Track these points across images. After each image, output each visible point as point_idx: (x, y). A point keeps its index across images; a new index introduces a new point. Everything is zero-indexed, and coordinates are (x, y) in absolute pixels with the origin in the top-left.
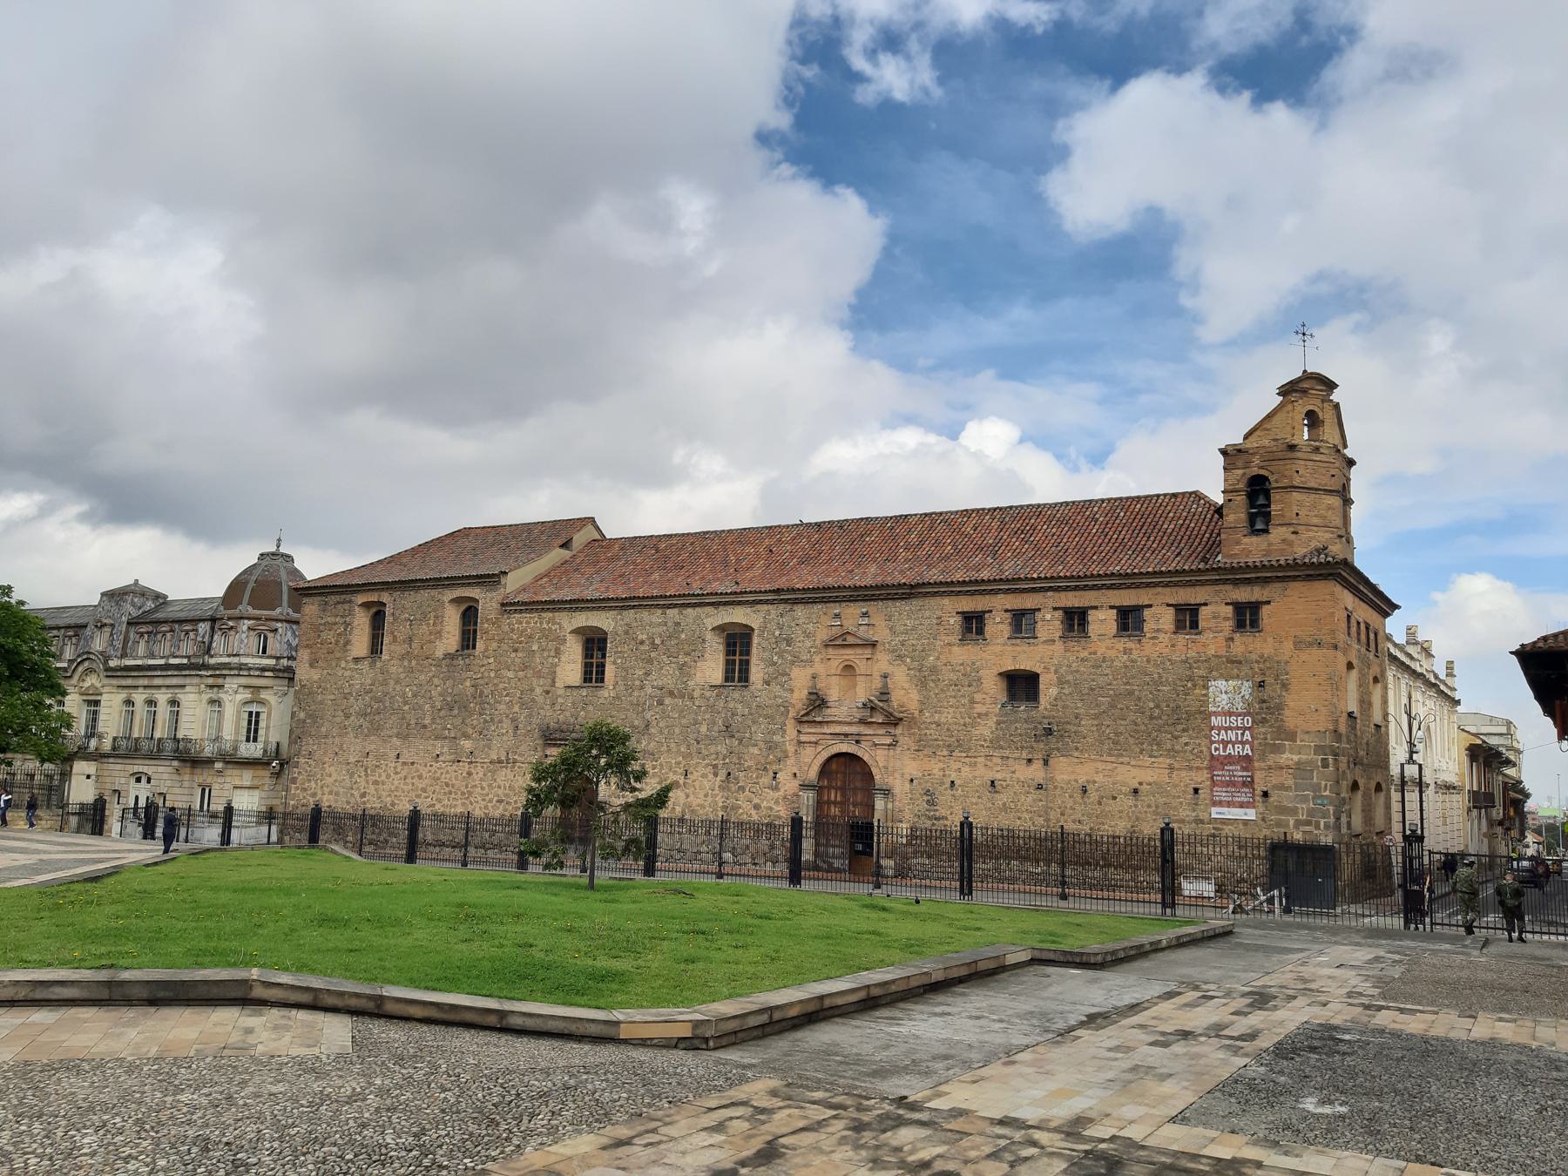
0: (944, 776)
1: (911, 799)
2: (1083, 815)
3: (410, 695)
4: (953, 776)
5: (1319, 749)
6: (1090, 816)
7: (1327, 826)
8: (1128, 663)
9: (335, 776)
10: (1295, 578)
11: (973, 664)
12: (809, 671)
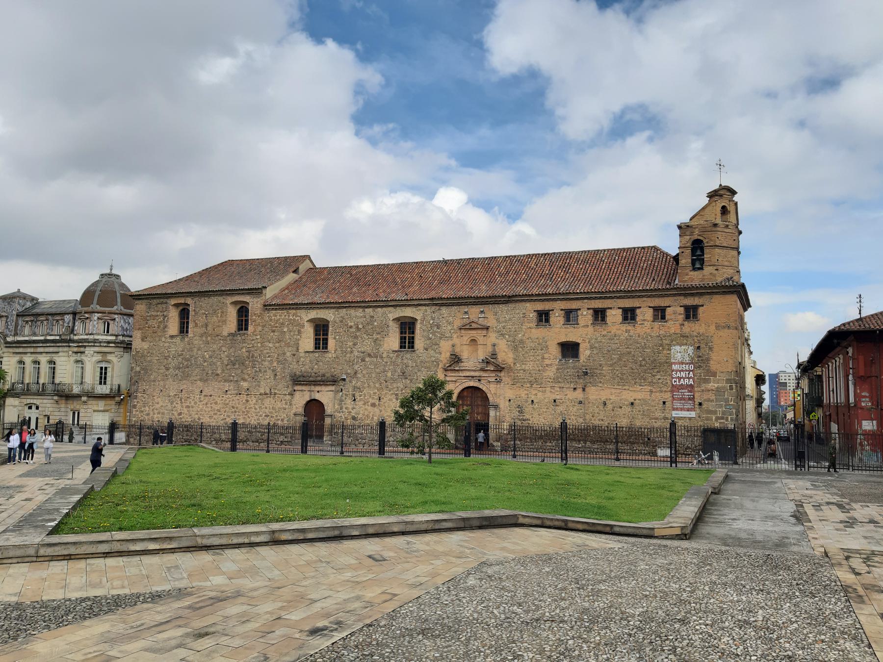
2: (604, 417)
3: (207, 356)
4: (533, 398)
5: (728, 381)
6: (607, 417)
7: (732, 419)
8: (628, 337)
9: (161, 404)
10: (716, 293)
11: (544, 338)
12: (450, 343)
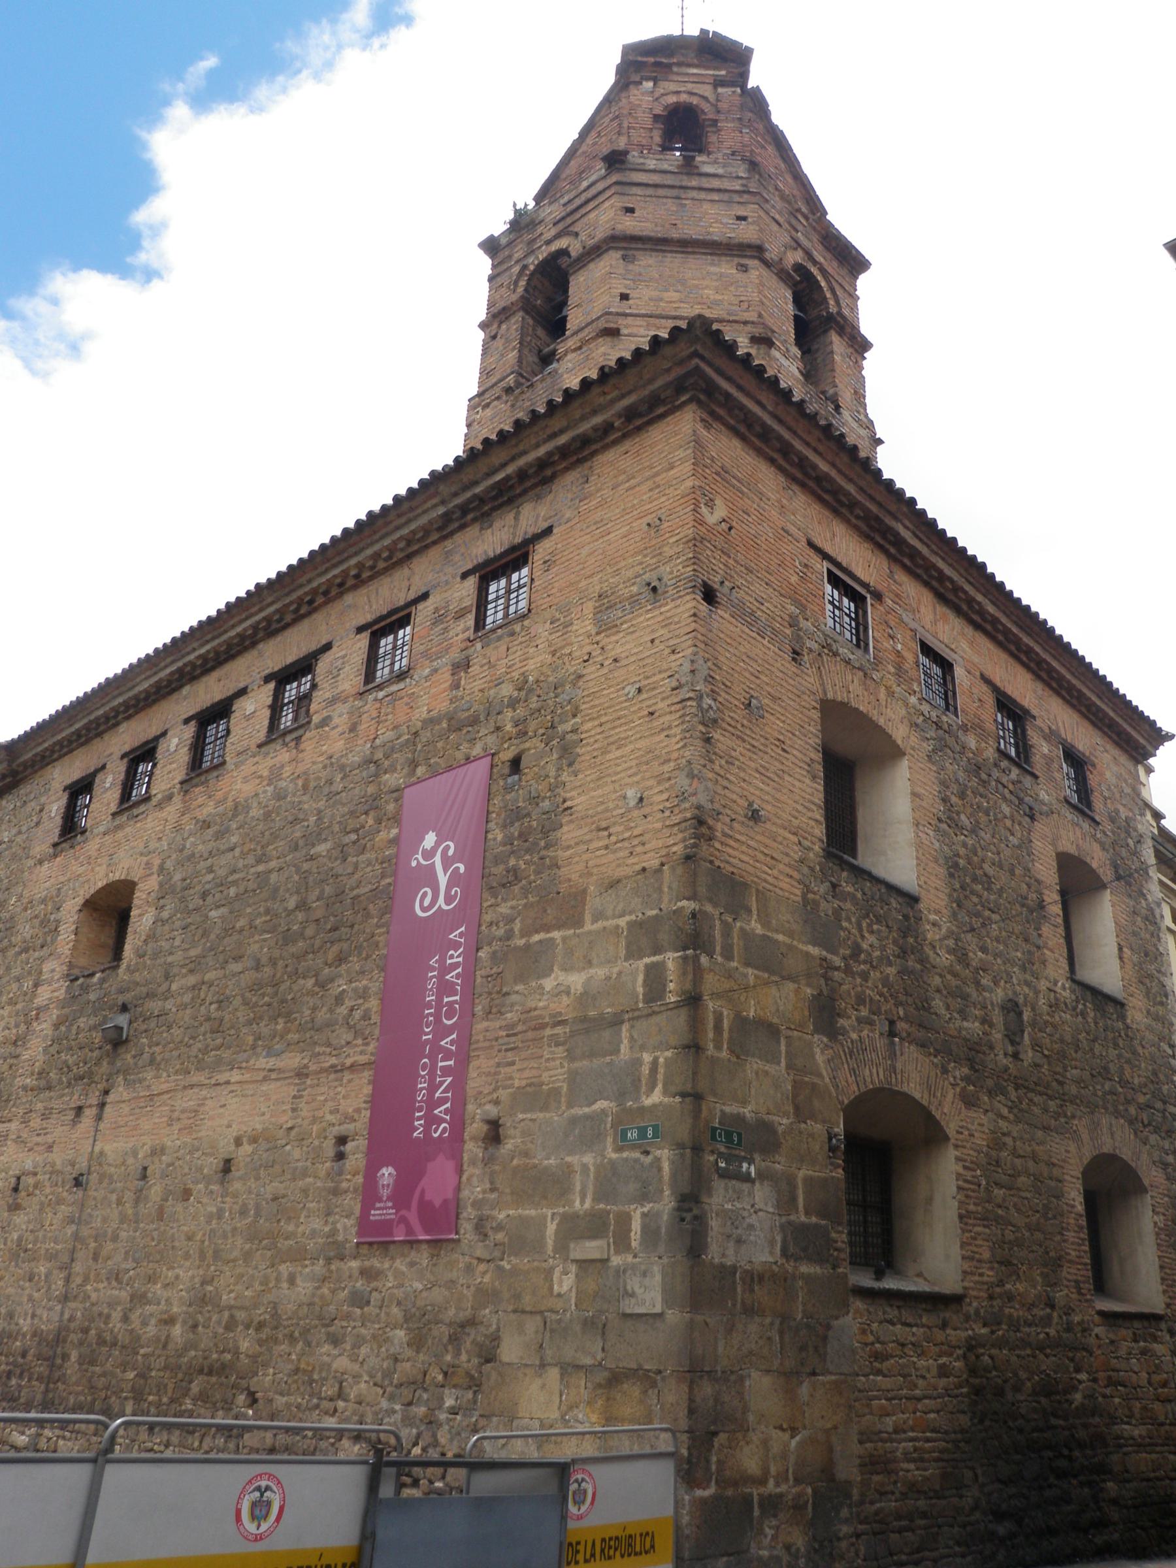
7: (650, 1234)
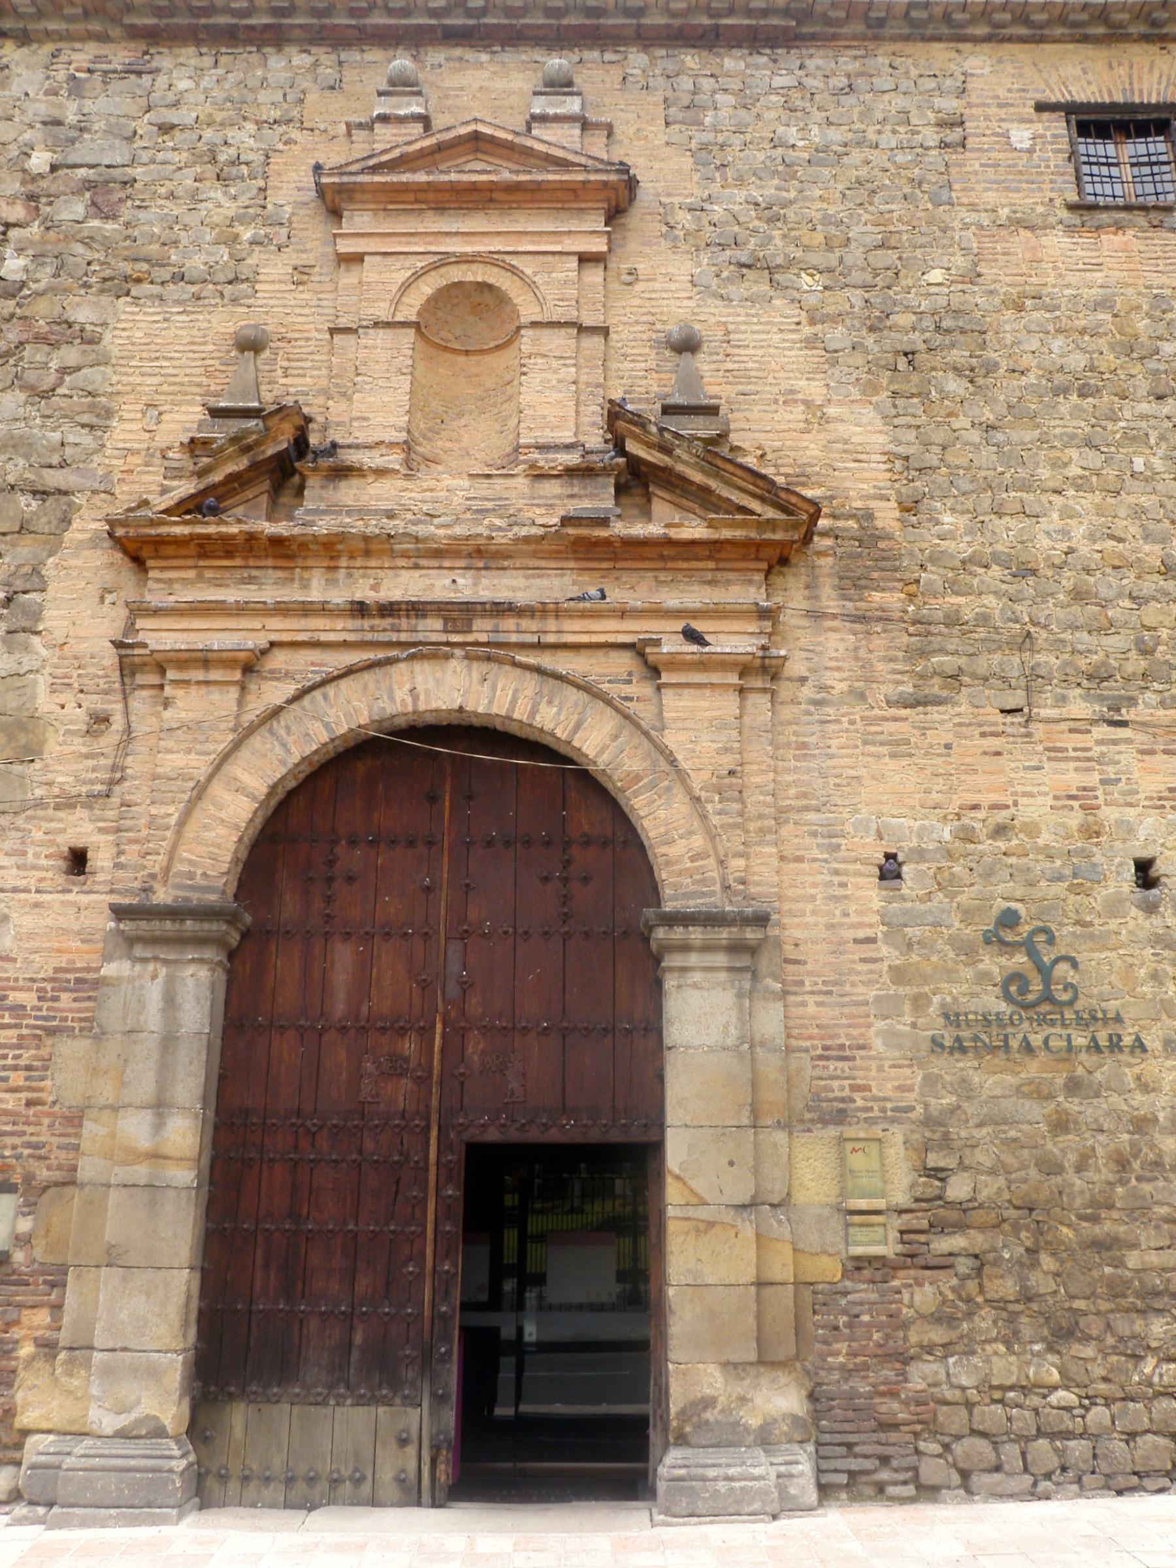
0: (1091, 832)
1: (899, 975)
